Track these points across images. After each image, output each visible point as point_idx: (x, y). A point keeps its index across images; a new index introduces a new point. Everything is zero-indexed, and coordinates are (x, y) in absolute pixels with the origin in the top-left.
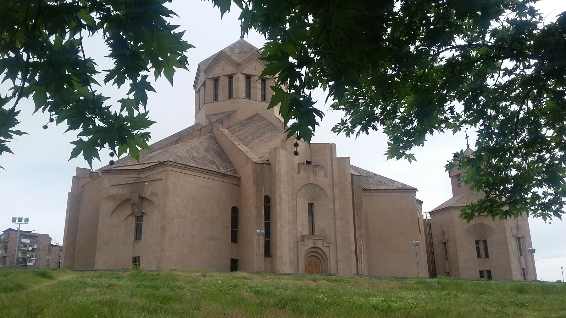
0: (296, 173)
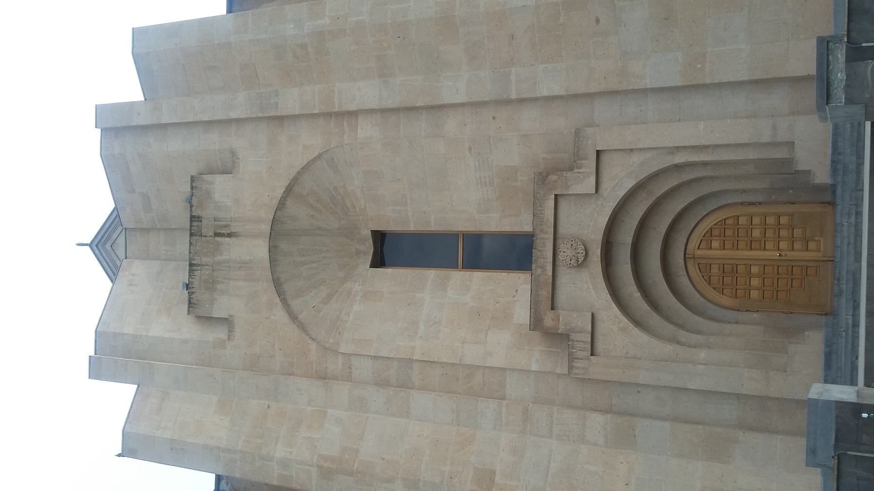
0: (228, 339)
